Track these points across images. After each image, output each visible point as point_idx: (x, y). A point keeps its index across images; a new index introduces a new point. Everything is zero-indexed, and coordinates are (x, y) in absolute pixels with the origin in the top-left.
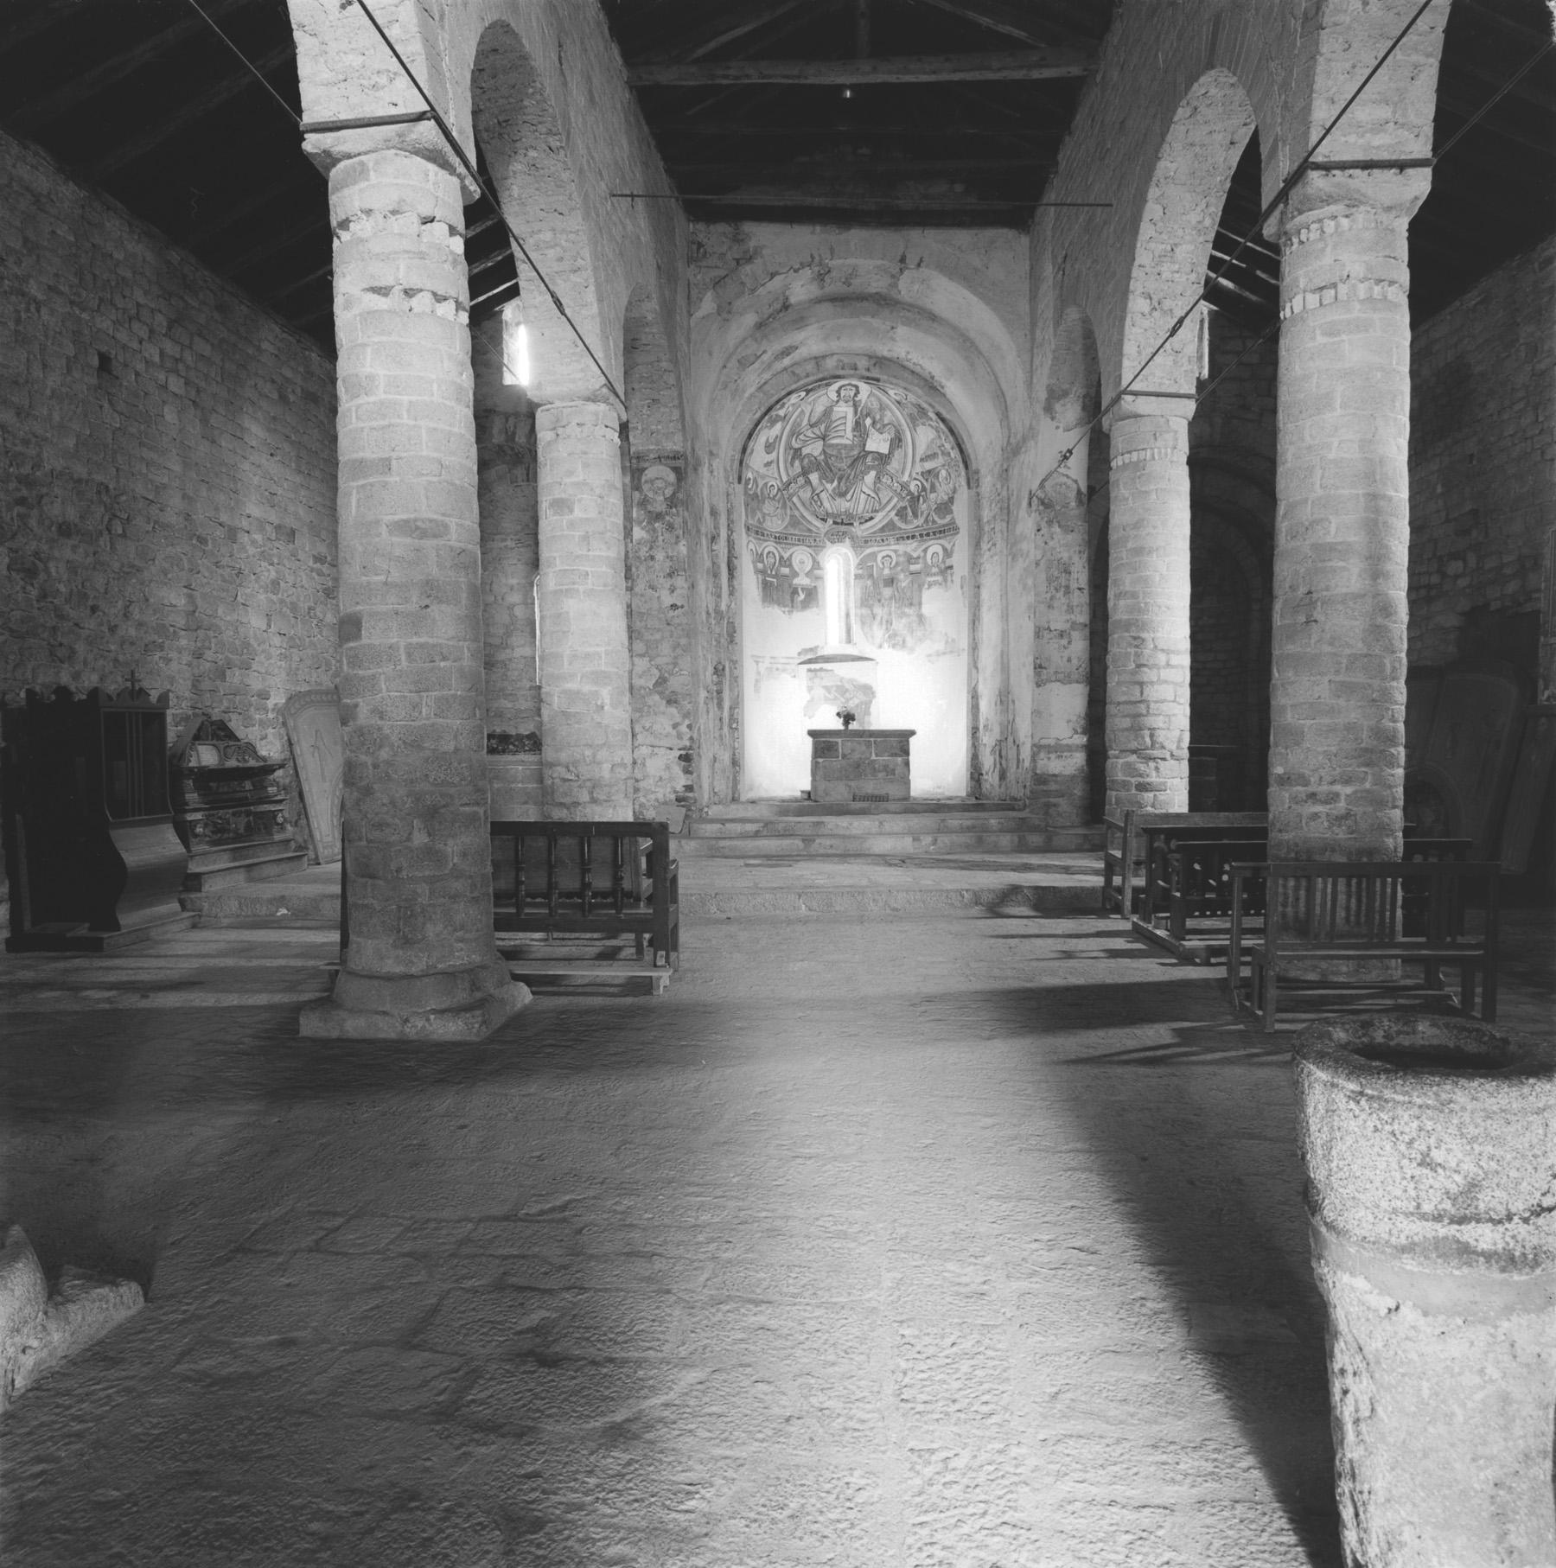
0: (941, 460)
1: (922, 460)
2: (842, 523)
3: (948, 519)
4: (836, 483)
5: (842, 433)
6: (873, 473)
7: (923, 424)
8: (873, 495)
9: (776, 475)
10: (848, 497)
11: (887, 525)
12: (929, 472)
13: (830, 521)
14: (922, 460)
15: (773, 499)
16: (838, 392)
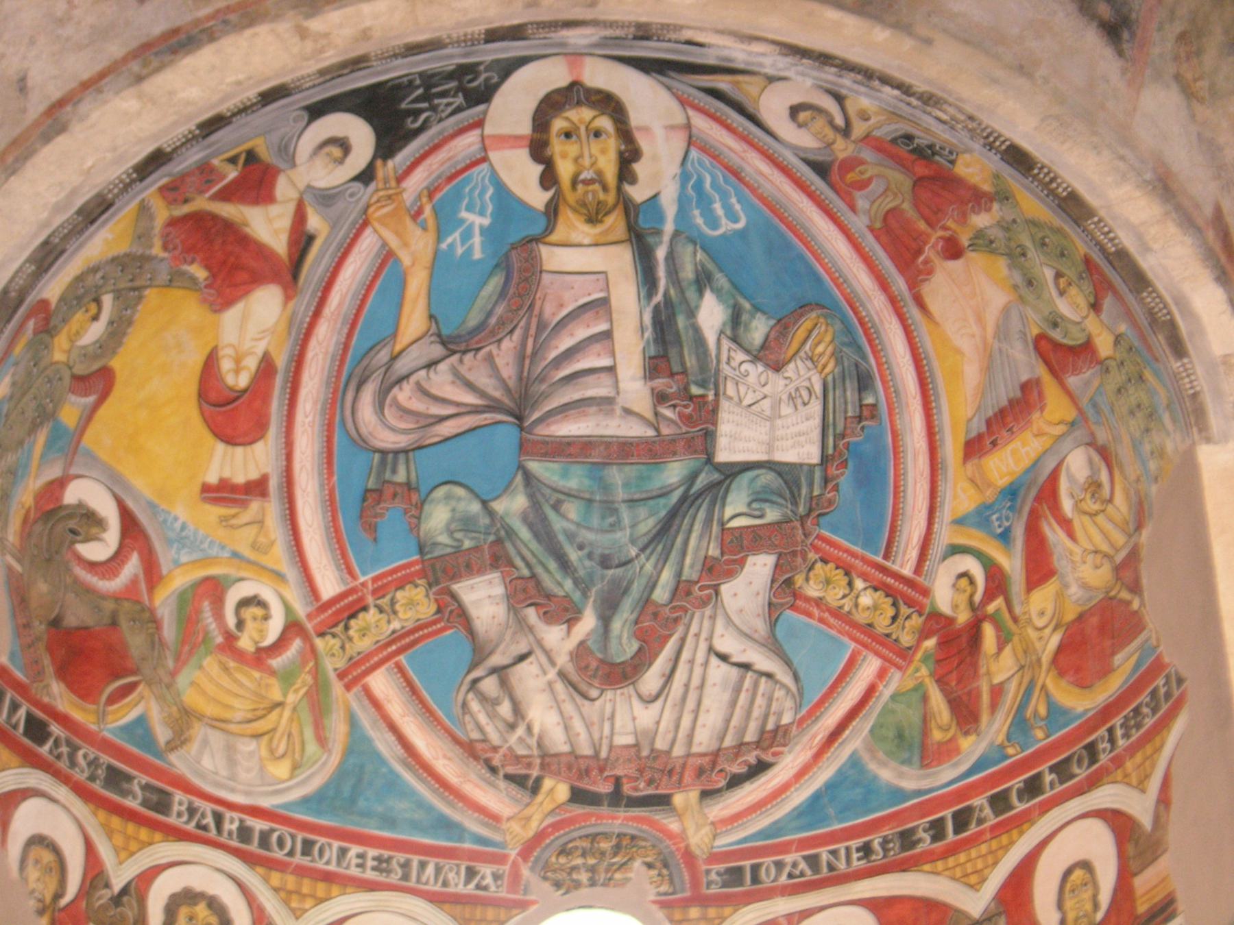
0: (1056, 407)
1: (974, 448)
2: (617, 798)
3: (1125, 663)
4: (588, 622)
5: (598, 388)
6: (760, 566)
7: (953, 251)
8: (763, 661)
9: (279, 556)
10: (651, 680)
11: (831, 787)
12: (1012, 492)
13: (557, 790)
14: (974, 448)
15: (260, 657)
16: (539, 149)
